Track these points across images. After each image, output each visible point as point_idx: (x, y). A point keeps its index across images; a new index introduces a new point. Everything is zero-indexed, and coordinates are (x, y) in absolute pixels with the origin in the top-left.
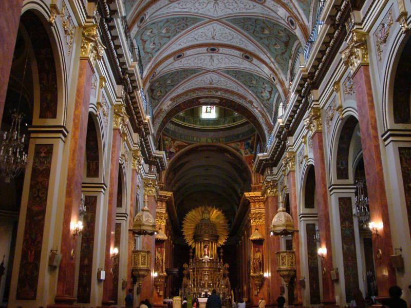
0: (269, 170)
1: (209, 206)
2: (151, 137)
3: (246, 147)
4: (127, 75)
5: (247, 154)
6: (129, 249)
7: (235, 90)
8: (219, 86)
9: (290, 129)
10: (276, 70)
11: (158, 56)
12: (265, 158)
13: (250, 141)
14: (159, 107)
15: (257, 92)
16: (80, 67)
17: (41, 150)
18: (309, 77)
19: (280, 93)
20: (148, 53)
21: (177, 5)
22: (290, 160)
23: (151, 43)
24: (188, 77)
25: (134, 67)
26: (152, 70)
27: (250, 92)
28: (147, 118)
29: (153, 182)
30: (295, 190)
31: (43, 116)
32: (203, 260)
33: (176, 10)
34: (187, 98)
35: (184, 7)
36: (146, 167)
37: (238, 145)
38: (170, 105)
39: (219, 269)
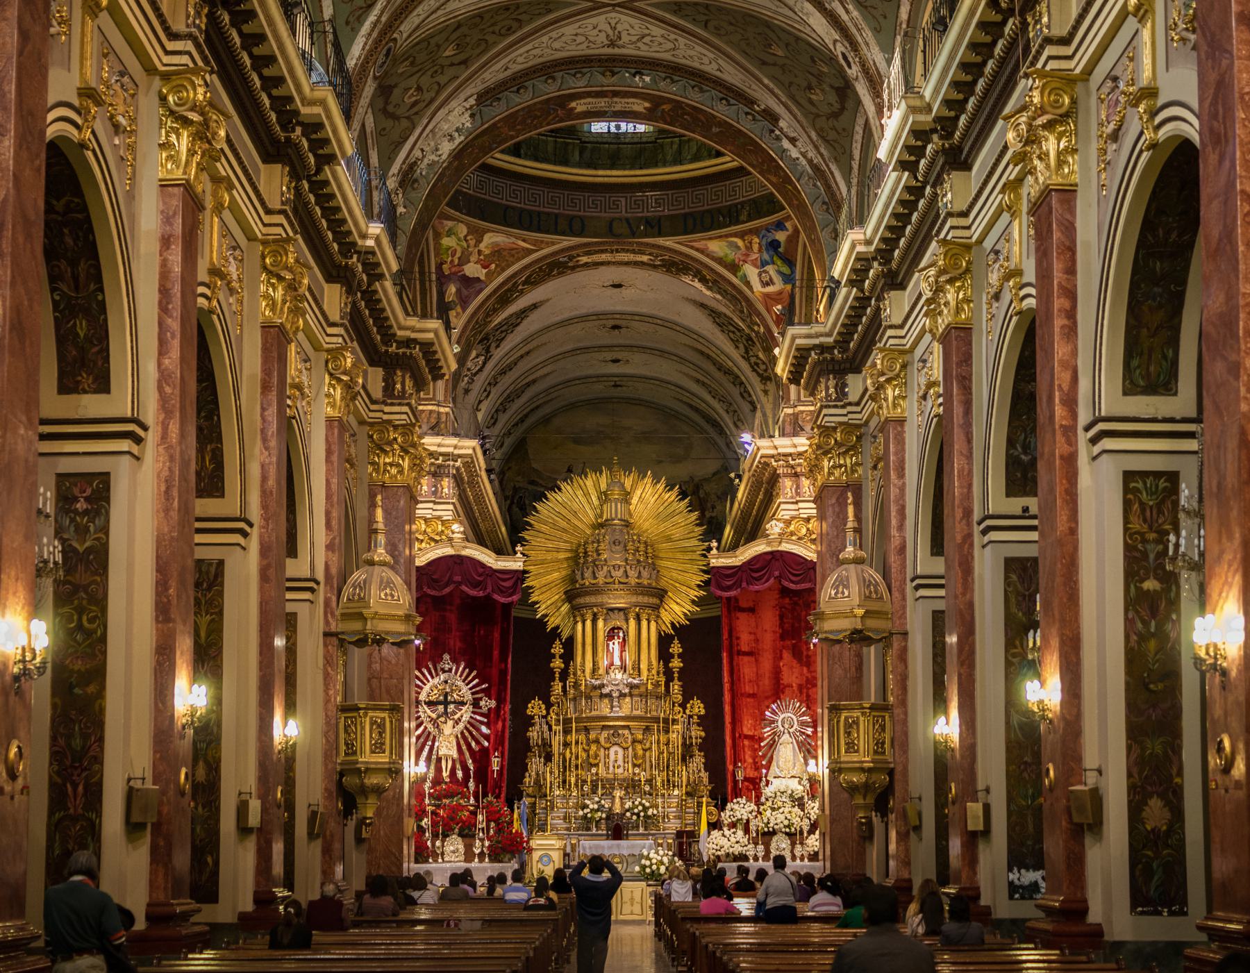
0: (832, 383)
1: (627, 469)
2: (388, 284)
3: (766, 257)
4: (299, 130)
5: (766, 284)
6: (327, 701)
7: (711, 69)
8: (644, 51)
9: (894, 265)
10: (854, 30)
12: (817, 341)
13: (781, 236)
15: (791, 84)
17: (76, 491)
18: (934, 131)
19: (870, 116)
22: (889, 381)
24: (520, 27)
25: (322, 103)
26: (383, 33)
27: (766, 81)
28: (371, 231)
29: (403, 434)
30: (902, 489)
31: (67, 386)
32: (602, 686)
34: (521, 100)
36: (375, 378)
37: (738, 248)
39: (667, 724)
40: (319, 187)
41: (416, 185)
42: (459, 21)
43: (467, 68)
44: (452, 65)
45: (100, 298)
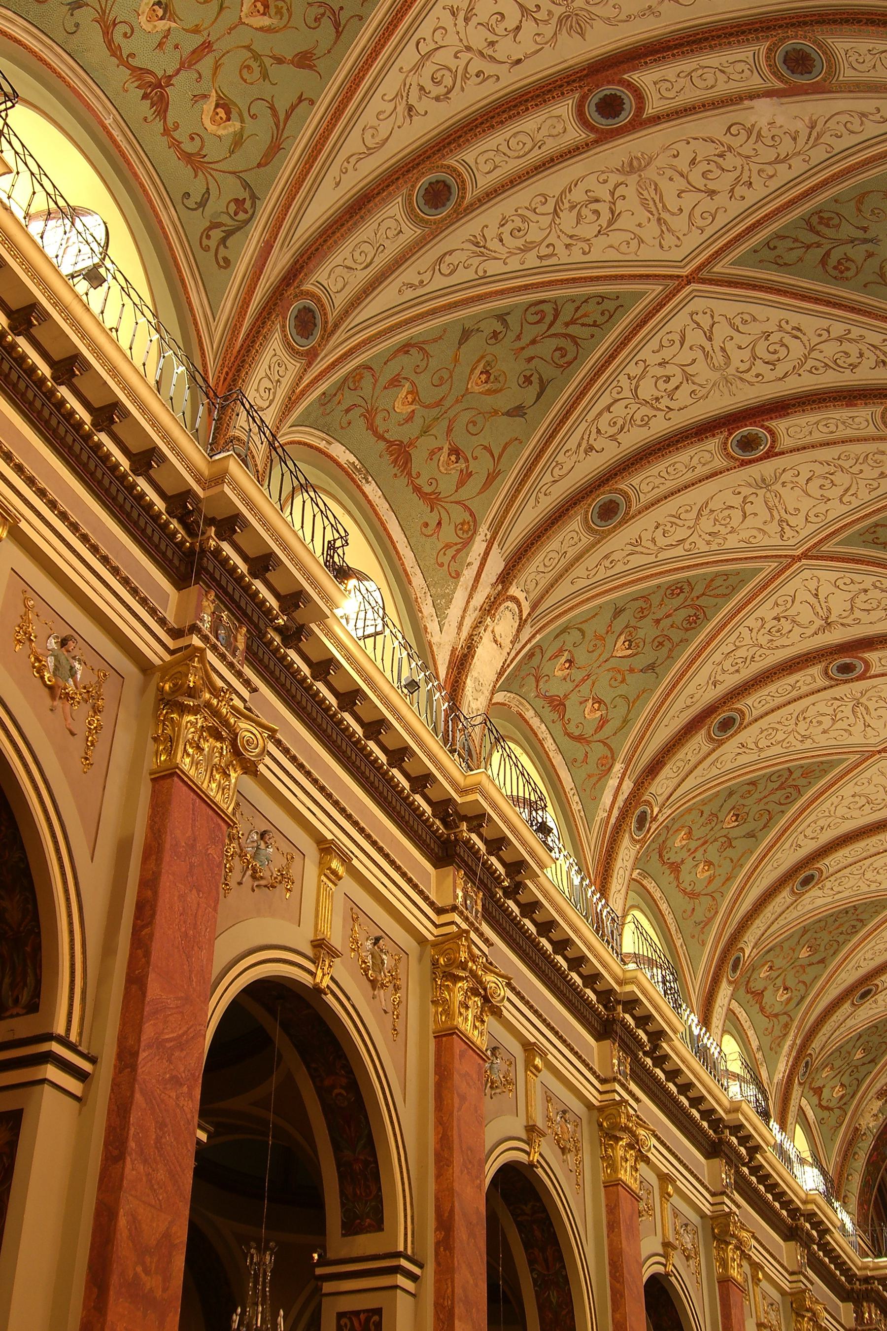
11: (806, 1013)
14: (849, 1126)
16: (607, 1205)
20: (776, 1016)
21: (820, 893)
23: (778, 990)
33: (819, 902)
35: (836, 889)
38: (880, 1111)
40: (756, 1170)
41: (856, 1157)
42: (859, 1033)
43: (876, 1064)
44: (864, 1064)
45: (564, 1273)
